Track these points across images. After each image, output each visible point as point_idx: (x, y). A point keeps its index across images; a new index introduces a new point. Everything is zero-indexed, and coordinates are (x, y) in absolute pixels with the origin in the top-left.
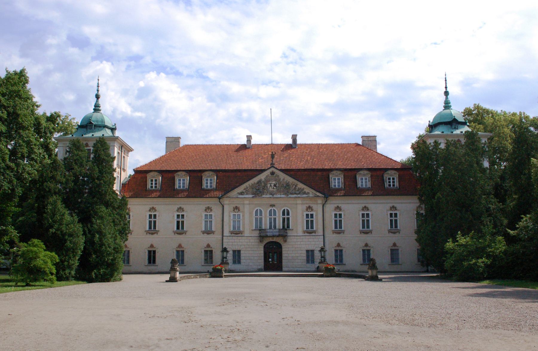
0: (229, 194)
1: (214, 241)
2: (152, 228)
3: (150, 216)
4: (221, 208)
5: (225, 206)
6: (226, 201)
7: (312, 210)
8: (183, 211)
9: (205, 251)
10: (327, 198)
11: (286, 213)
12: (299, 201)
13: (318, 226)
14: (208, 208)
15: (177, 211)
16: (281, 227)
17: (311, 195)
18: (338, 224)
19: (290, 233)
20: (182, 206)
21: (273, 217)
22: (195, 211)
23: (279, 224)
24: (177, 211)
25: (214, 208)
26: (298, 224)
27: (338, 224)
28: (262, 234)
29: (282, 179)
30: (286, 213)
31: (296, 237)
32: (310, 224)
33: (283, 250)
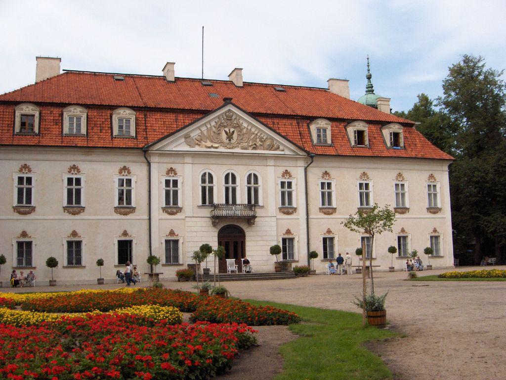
0: (159, 146)
1: (134, 227)
2: (74, 198)
3: (21, 180)
4: (145, 168)
5: (151, 164)
6: (154, 159)
7: (290, 176)
8: (79, 171)
9: (120, 242)
10: (312, 157)
11: (253, 179)
12: (271, 162)
13: (298, 200)
14: (125, 168)
15: (69, 172)
16: (246, 203)
17: (287, 152)
18: (327, 197)
19: (259, 212)
20: (76, 164)
21: (230, 184)
22: (101, 175)
23: (242, 198)
24: (69, 172)
25: (133, 168)
26: (270, 197)
27: (327, 197)
28: (218, 213)
29: (245, 125)
30: (253, 179)
31: (267, 219)
32: (286, 197)
33: (246, 237)
